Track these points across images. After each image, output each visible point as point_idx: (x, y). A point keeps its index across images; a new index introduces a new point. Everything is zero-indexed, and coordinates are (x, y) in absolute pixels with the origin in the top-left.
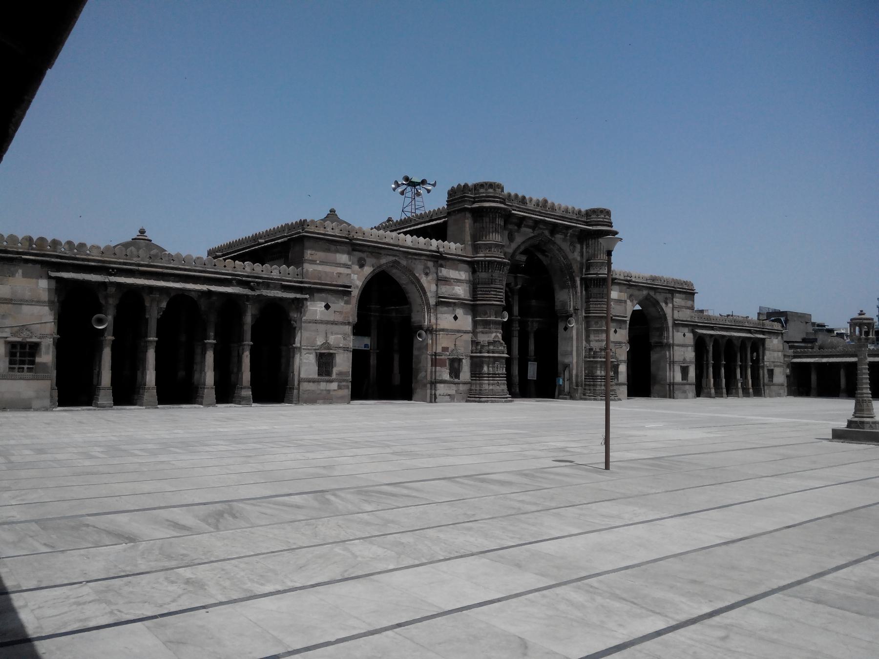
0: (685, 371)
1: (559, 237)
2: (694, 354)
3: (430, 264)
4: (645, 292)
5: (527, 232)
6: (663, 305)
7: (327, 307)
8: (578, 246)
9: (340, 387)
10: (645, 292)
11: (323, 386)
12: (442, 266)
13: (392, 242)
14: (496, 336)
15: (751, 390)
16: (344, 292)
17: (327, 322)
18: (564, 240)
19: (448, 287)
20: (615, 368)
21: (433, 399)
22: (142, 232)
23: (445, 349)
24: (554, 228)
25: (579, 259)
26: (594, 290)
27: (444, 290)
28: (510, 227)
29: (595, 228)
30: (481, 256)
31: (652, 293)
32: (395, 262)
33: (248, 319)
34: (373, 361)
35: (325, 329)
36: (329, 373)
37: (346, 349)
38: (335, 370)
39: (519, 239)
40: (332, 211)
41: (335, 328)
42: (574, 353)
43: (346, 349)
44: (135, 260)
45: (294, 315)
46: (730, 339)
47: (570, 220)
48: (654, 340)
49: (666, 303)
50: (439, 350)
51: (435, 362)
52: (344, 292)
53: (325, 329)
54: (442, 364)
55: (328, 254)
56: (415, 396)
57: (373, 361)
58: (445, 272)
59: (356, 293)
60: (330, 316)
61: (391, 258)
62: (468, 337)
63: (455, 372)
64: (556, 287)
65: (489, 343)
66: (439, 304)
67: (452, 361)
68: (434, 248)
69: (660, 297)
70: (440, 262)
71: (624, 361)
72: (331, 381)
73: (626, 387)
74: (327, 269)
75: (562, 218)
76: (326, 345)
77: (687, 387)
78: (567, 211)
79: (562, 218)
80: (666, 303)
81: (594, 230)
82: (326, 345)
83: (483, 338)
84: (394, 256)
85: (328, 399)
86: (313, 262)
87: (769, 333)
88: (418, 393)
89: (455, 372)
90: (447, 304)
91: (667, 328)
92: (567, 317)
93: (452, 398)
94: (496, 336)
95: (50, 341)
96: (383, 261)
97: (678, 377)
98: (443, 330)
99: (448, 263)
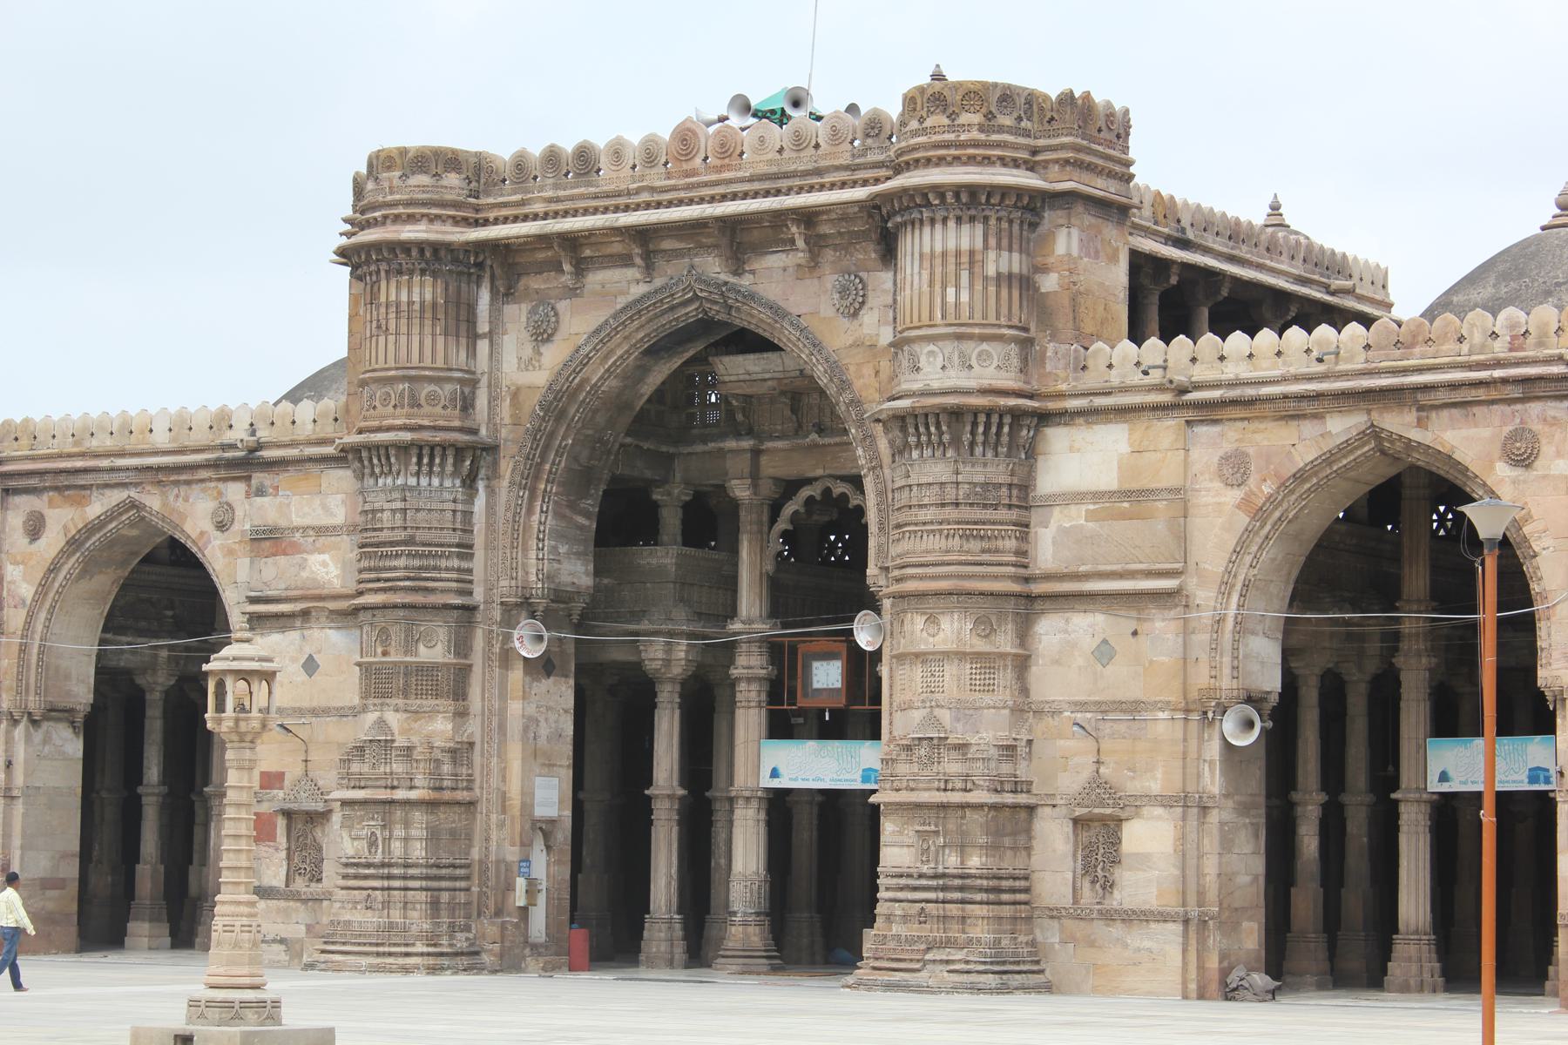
3: (235, 491)
4: (1341, 426)
6: (1502, 475)
8: (887, 276)
10: (1341, 426)
12: (260, 492)
13: (109, 443)
14: (381, 723)
19: (282, 560)
28: (535, 283)
31: (1399, 423)
32: (133, 505)
39: (578, 323)
47: (813, 178)
49: (1523, 459)
61: (116, 497)
63: (306, 859)
68: (239, 434)
69: (1465, 441)
70: (258, 478)
71: (1165, 802)
73: (1177, 928)
79: (772, 182)
84: (124, 485)
89: (306, 859)
94: (381, 723)
96: (96, 508)
99: (283, 476)
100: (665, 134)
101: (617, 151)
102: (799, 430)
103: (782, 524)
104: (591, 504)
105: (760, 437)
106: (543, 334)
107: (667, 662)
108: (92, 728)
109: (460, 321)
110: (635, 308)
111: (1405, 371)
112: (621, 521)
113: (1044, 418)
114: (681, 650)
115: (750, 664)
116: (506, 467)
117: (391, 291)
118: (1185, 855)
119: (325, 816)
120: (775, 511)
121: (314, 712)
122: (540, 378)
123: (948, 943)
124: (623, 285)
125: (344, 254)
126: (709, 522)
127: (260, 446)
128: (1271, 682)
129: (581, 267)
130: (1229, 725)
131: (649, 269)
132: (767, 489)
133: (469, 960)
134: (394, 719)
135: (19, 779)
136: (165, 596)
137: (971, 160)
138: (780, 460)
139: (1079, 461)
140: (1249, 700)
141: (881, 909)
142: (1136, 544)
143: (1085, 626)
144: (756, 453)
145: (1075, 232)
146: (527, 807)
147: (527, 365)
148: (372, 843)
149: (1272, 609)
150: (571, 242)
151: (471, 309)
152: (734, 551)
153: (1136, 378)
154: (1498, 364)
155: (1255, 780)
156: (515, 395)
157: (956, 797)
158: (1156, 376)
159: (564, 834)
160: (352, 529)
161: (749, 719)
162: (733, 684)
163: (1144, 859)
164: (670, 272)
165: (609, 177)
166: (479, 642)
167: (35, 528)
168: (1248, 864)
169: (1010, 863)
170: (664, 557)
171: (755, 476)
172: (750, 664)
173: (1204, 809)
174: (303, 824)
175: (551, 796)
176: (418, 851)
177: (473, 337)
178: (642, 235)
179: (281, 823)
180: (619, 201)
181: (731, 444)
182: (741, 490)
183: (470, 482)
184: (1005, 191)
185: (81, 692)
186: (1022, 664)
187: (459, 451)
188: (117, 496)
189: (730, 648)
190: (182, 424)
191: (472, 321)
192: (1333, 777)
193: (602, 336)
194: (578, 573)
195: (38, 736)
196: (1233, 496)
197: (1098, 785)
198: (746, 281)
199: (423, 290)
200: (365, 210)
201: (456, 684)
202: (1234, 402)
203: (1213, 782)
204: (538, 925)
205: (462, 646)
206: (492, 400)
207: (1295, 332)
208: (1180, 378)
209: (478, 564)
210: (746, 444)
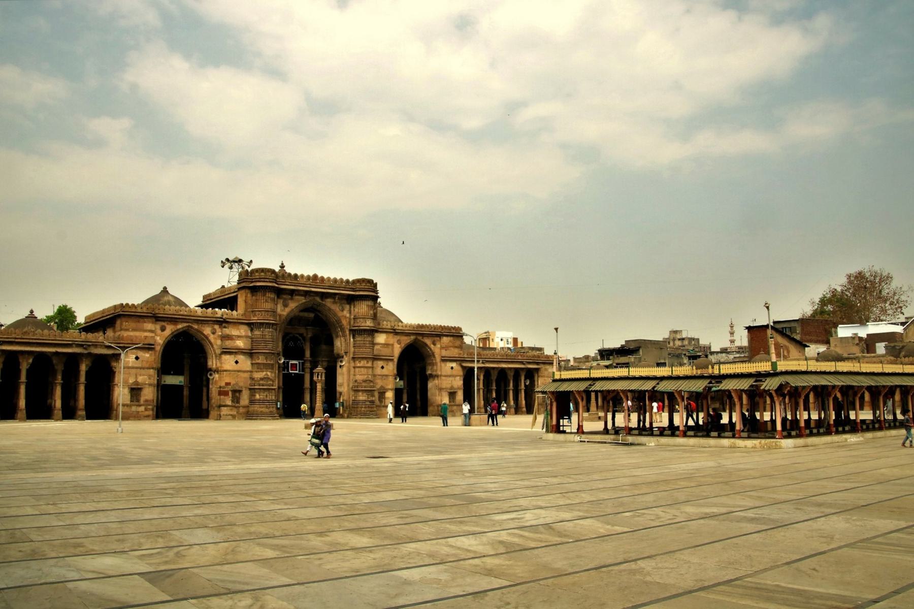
0: (452, 395)
1: (328, 302)
2: (462, 382)
3: (216, 327)
4: (413, 337)
7: (137, 358)
8: (348, 306)
9: (146, 410)
10: (413, 337)
11: (134, 408)
15: (524, 409)
16: (149, 347)
17: (137, 368)
18: (335, 303)
20: (382, 394)
21: (219, 418)
22: (32, 312)
24: (324, 296)
25: (348, 315)
26: (358, 338)
27: (228, 343)
29: (357, 293)
30: (254, 319)
31: (420, 338)
32: (188, 326)
33: (83, 368)
34: (186, 392)
35: (135, 370)
36: (138, 401)
37: (150, 385)
38: (142, 399)
39: (293, 305)
40: (165, 288)
41: (143, 371)
42: (346, 384)
43: (150, 385)
44: (14, 336)
45: (114, 364)
46: (502, 371)
48: (429, 372)
49: (434, 344)
50: (223, 384)
51: (222, 393)
53: (135, 370)
54: (225, 393)
55: (139, 325)
56: (211, 416)
57: (186, 392)
58: (227, 331)
59: (158, 348)
60: (138, 364)
61: (185, 325)
62: (247, 375)
64: (334, 336)
65: (262, 379)
67: (234, 392)
68: (219, 315)
69: (428, 341)
72: (140, 406)
74: (137, 334)
75: (331, 287)
76: (136, 383)
77: (455, 408)
78: (335, 280)
80: (434, 344)
81: (364, 292)
82: (136, 383)
83: (258, 375)
85: (137, 417)
86: (127, 330)
87: (544, 363)
88: (213, 413)
90: (230, 353)
91: (436, 364)
92: (339, 357)
93: (234, 417)
96: (180, 326)
97: (446, 400)
98: (226, 371)
99: (231, 325)
101: (302, 276)
106: (285, 306)
119: (240, 391)
121: (239, 371)
122: (285, 313)
134: (269, 374)
139: (381, 338)
142: (385, 352)
143: (380, 363)
156: (280, 315)
160: (247, 337)
174: (236, 393)
179: (230, 393)
197: (382, 387)
199: (273, 296)
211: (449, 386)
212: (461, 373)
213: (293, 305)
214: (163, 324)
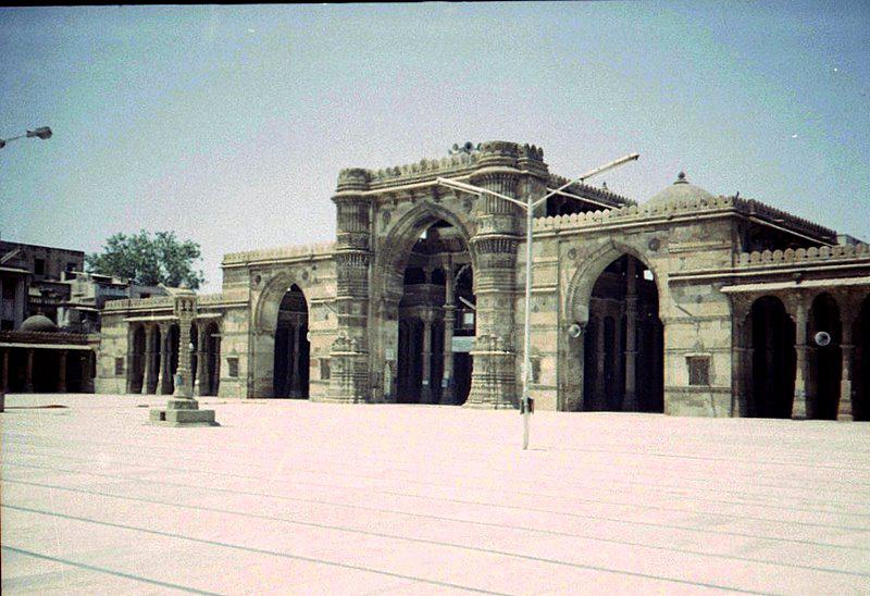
2: (729, 332)
3: (309, 269)
4: (602, 240)
5: (407, 206)
12: (314, 268)
23: (317, 350)
28: (385, 207)
31: (619, 239)
52: (247, 306)
63: (326, 373)
66: (314, 305)
68: (309, 252)
69: (638, 243)
73: (555, 392)
76: (234, 352)
77: (706, 396)
82: (234, 352)
94: (342, 334)
95: (125, 358)
100: (418, 163)
102: (462, 250)
103: (458, 277)
104: (403, 271)
105: (452, 251)
107: (427, 317)
108: (277, 338)
109: (363, 218)
110: (410, 213)
111: (621, 223)
112: (412, 276)
113: (520, 241)
114: (431, 313)
115: (449, 318)
116: (377, 260)
117: (344, 210)
118: (559, 369)
120: (456, 273)
122: (386, 234)
123: (489, 395)
124: (407, 206)
125: (335, 199)
126: (439, 278)
127: (313, 256)
128: (586, 318)
129: (396, 203)
130: (571, 329)
131: (414, 201)
132: (455, 268)
133: (369, 400)
134: (346, 333)
135: (256, 350)
136: (295, 302)
137: (497, 165)
138: (457, 257)
140: (577, 323)
141: (472, 385)
144: (450, 257)
145: (529, 186)
146: (384, 357)
147: (383, 230)
148: (340, 366)
149: (585, 295)
150: (392, 194)
151: (367, 214)
152: (445, 284)
153: (545, 229)
154: (649, 220)
155: (580, 348)
157: (493, 352)
158: (550, 228)
159: (395, 365)
161: (448, 332)
162: (444, 323)
163: (546, 371)
164: (419, 201)
165: (404, 175)
166: (370, 310)
167: (259, 279)
168: (576, 374)
169: (508, 371)
170: (426, 287)
171: (450, 262)
172: (449, 318)
173: (564, 355)
175: (391, 354)
176: (352, 367)
177: (368, 224)
178: (411, 191)
179: (319, 362)
180: (403, 182)
181: (443, 254)
182: (447, 268)
183: (367, 265)
184: (507, 173)
185: (273, 325)
186: (513, 315)
187: (363, 256)
188: (278, 271)
189: (444, 311)
190: (294, 250)
191: (367, 217)
192: (609, 348)
193: (402, 220)
194: (399, 291)
195: (261, 338)
196: (573, 262)
198: (440, 204)
199: (354, 210)
200: (341, 188)
201: (364, 324)
202: (572, 235)
203: (567, 348)
204: (388, 388)
205: (365, 312)
206: (373, 240)
207: (590, 213)
208: (557, 227)
209: (370, 288)
210: (447, 254)
211: (691, 343)
212: (725, 310)
213: (395, 218)
214: (260, 273)
